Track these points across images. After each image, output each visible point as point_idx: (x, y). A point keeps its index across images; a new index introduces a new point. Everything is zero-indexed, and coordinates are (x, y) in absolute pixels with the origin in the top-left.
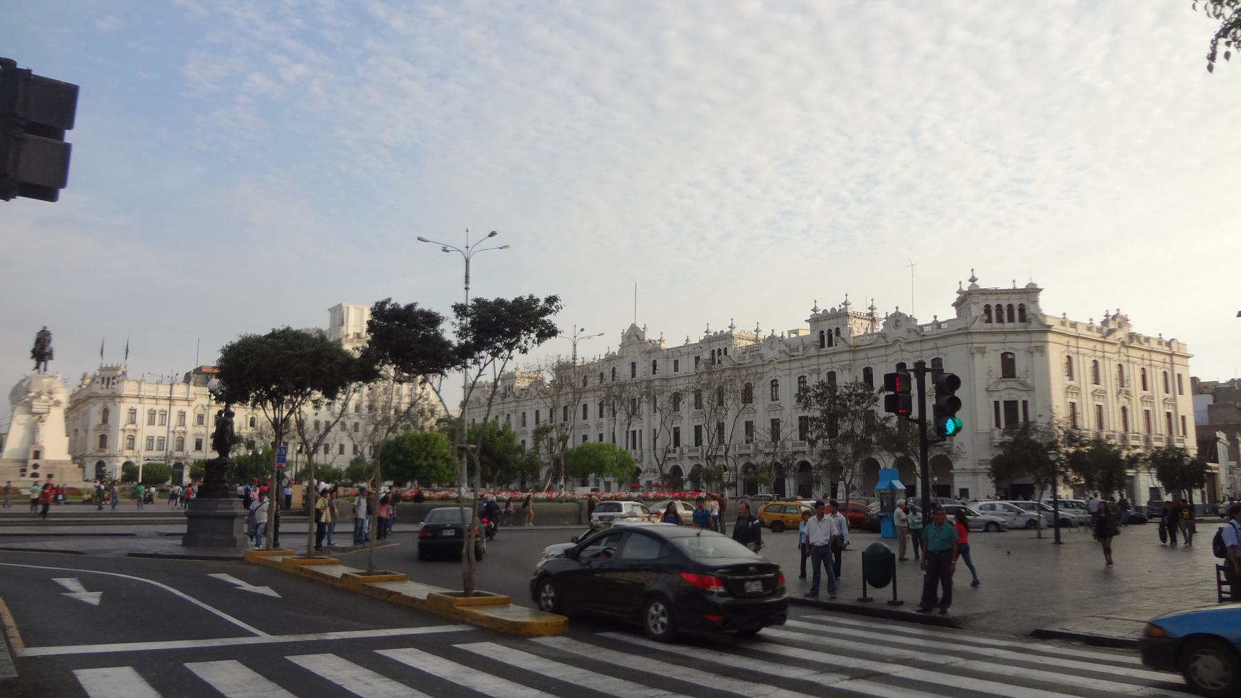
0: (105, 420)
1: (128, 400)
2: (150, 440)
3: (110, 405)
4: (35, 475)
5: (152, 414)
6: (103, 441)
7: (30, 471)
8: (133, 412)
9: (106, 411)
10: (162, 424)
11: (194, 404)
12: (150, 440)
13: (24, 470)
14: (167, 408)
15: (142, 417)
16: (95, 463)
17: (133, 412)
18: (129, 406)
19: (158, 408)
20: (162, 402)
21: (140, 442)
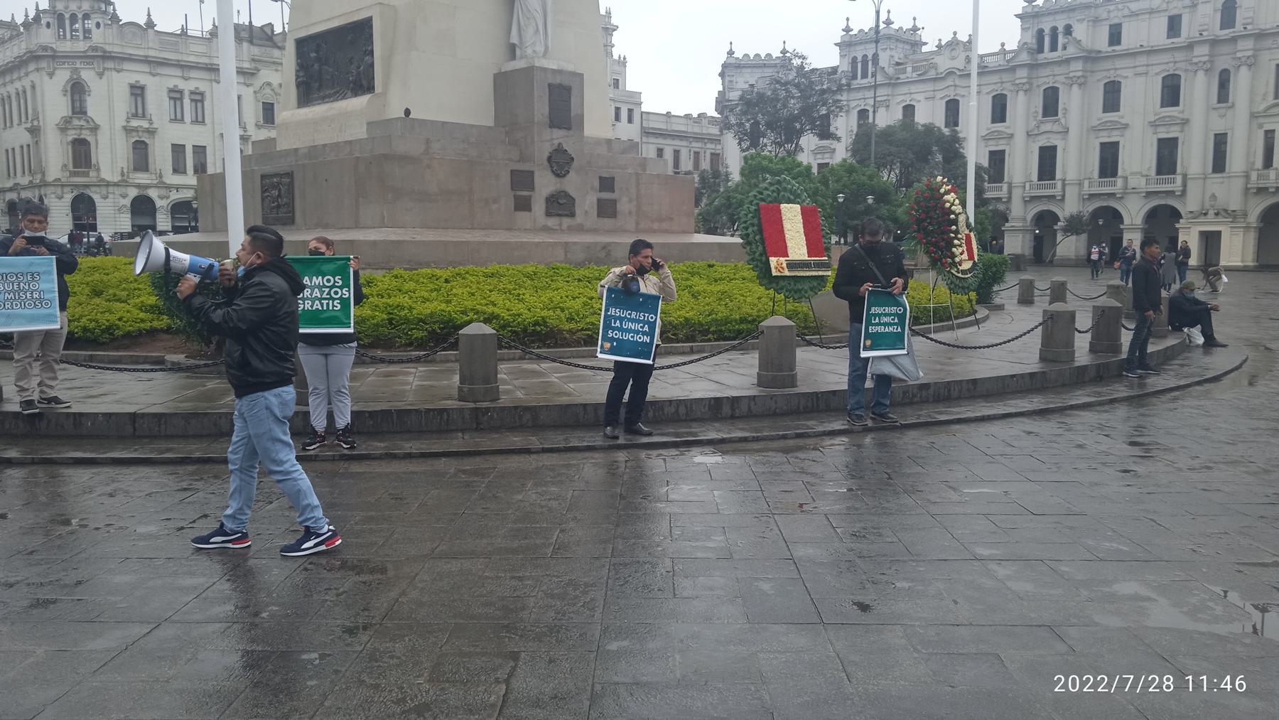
0: (79, 110)
1: (127, 66)
2: (178, 150)
3: (88, 75)
4: (560, 205)
5: (176, 96)
6: (81, 153)
7: (545, 184)
8: (138, 91)
9: (77, 90)
10: (199, 120)
11: (258, 83)
12: (178, 150)
13: (522, 180)
14: (203, 86)
15: (157, 103)
16: (69, 197)
17: (138, 91)
18: (133, 78)
19: (187, 86)
20: (194, 74)
21: (161, 157)
